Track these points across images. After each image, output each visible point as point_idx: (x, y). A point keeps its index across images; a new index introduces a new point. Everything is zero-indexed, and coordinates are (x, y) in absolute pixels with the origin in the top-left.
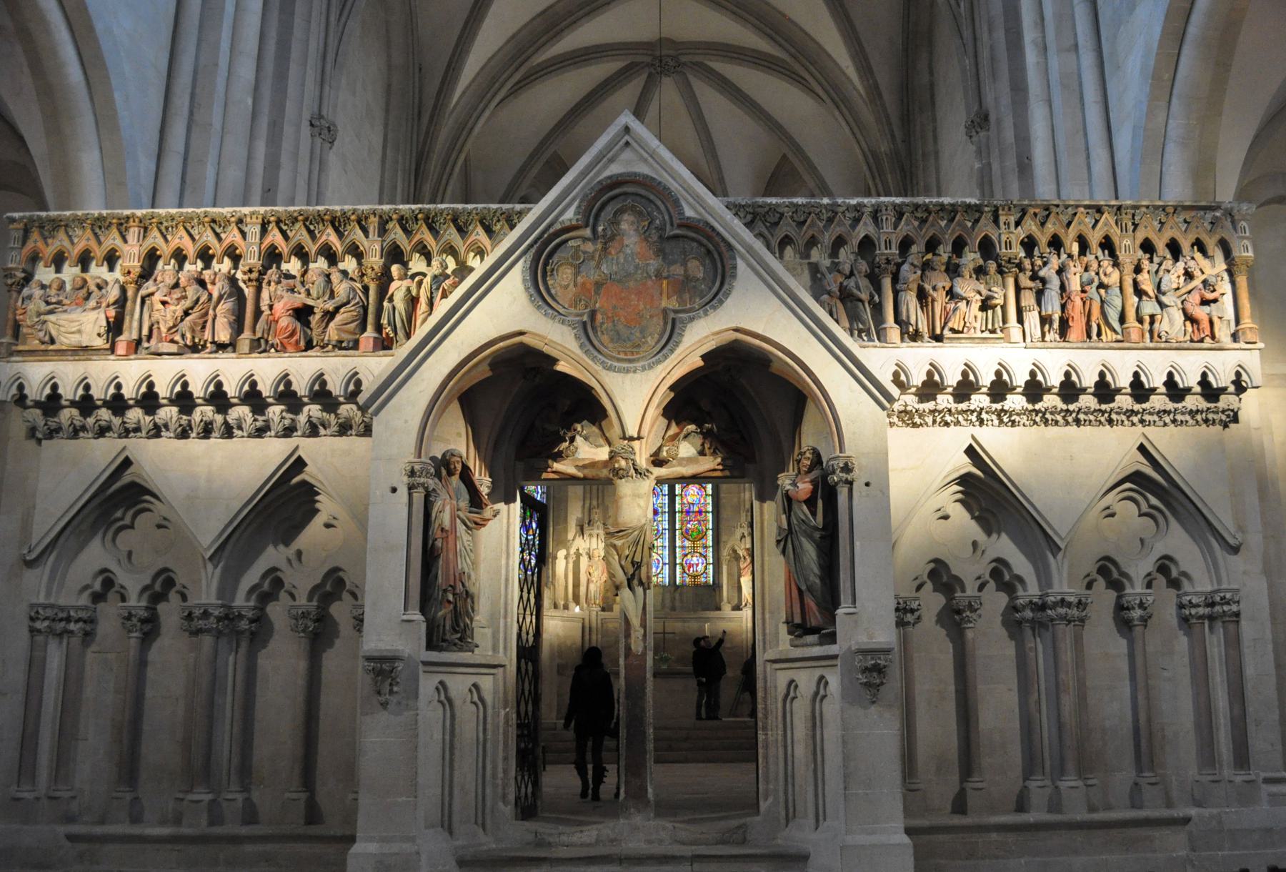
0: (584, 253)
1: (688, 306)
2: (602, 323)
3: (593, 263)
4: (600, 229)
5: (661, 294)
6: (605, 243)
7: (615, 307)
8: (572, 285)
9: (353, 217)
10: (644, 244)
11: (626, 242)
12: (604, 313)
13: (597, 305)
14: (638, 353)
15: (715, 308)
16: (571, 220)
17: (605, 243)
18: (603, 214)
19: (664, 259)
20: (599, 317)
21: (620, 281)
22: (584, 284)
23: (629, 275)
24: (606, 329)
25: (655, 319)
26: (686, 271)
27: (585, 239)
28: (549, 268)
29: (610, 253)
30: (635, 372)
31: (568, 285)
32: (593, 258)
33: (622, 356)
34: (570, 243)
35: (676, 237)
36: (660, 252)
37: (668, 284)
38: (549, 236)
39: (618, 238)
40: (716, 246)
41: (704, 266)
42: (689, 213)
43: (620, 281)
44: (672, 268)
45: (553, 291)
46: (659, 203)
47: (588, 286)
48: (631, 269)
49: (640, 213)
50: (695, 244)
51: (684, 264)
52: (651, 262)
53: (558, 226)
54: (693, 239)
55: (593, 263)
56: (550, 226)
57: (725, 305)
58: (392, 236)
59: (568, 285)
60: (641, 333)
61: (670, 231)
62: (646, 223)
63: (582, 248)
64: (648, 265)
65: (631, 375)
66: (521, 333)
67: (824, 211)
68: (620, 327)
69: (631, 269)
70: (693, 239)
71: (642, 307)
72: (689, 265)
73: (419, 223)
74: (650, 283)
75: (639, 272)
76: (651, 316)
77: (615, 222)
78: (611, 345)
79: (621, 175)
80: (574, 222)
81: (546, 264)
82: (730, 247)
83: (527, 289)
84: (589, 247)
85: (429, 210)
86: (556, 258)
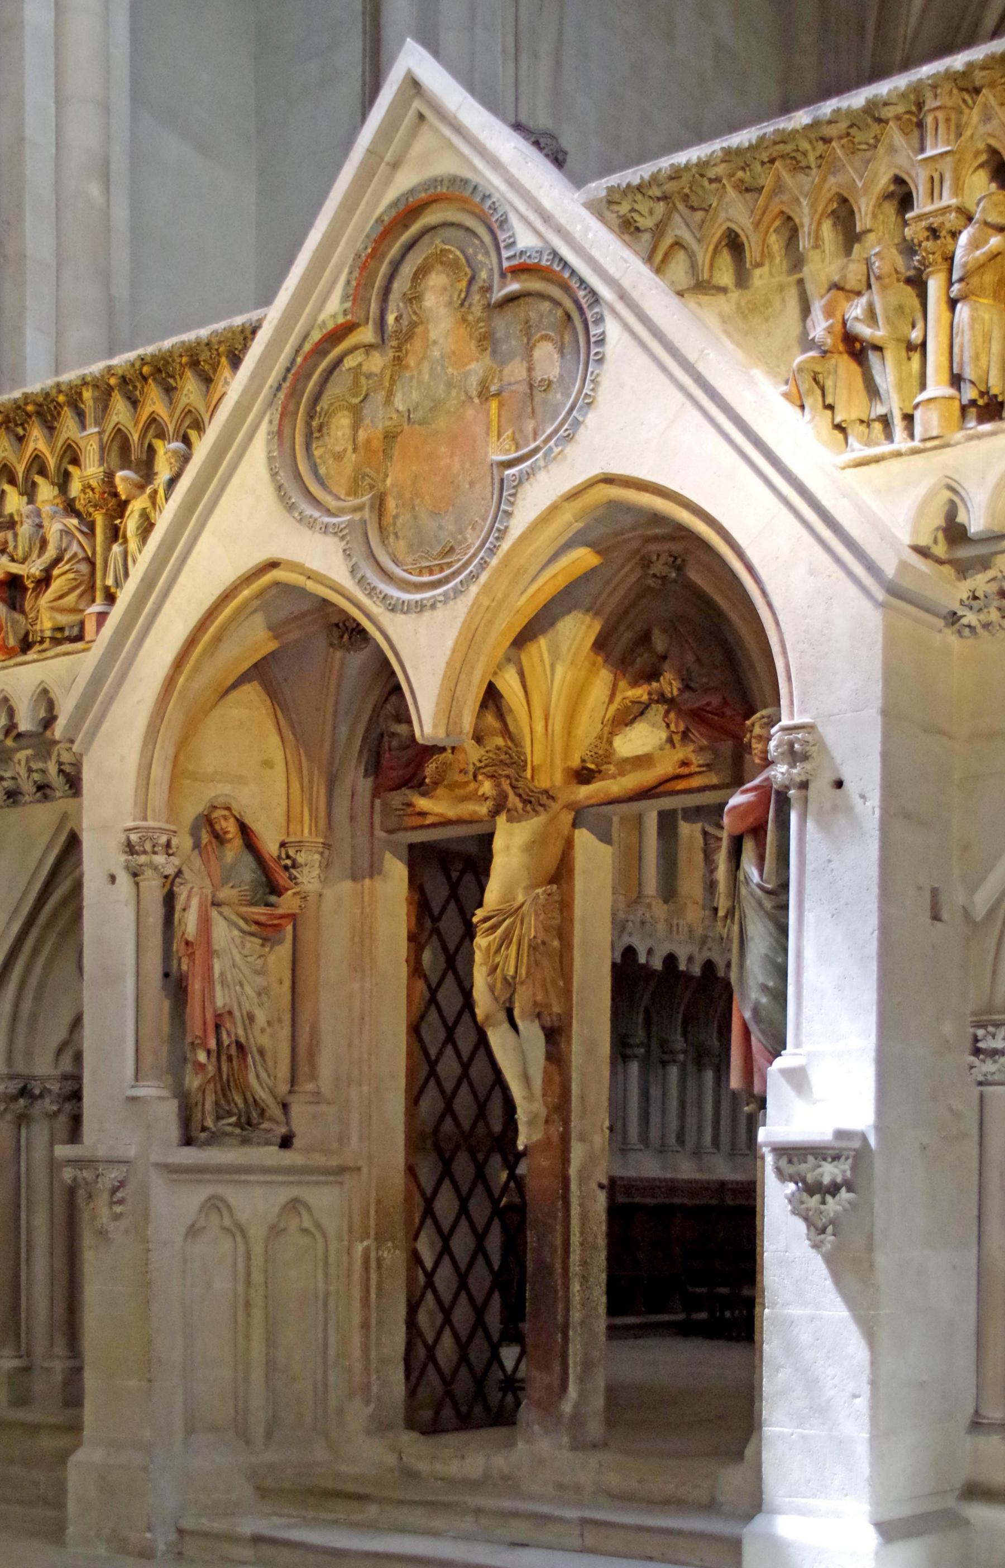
0: (368, 376)
3: (380, 397)
5: (488, 434)
6: (399, 348)
9: (61, 398)
11: (433, 336)
12: (400, 496)
14: (450, 565)
15: (569, 438)
16: (334, 316)
17: (399, 348)
19: (494, 352)
20: (391, 503)
21: (422, 422)
22: (368, 441)
23: (437, 405)
27: (369, 348)
29: (407, 367)
30: (433, 606)
31: (345, 450)
33: (426, 578)
34: (349, 362)
35: (512, 299)
36: (487, 341)
37: (501, 405)
38: (305, 359)
39: (419, 330)
42: (525, 240)
43: (422, 422)
45: (322, 470)
48: (440, 391)
50: (546, 306)
52: (473, 366)
53: (316, 336)
56: (305, 337)
59: (345, 450)
62: (464, 284)
65: (427, 615)
67: (805, 145)
69: (440, 391)
71: (456, 467)
72: (537, 354)
75: (454, 393)
76: (472, 484)
77: (414, 298)
79: (412, 191)
80: (341, 320)
82: (595, 298)
83: (274, 475)
84: (376, 363)
86: (324, 404)
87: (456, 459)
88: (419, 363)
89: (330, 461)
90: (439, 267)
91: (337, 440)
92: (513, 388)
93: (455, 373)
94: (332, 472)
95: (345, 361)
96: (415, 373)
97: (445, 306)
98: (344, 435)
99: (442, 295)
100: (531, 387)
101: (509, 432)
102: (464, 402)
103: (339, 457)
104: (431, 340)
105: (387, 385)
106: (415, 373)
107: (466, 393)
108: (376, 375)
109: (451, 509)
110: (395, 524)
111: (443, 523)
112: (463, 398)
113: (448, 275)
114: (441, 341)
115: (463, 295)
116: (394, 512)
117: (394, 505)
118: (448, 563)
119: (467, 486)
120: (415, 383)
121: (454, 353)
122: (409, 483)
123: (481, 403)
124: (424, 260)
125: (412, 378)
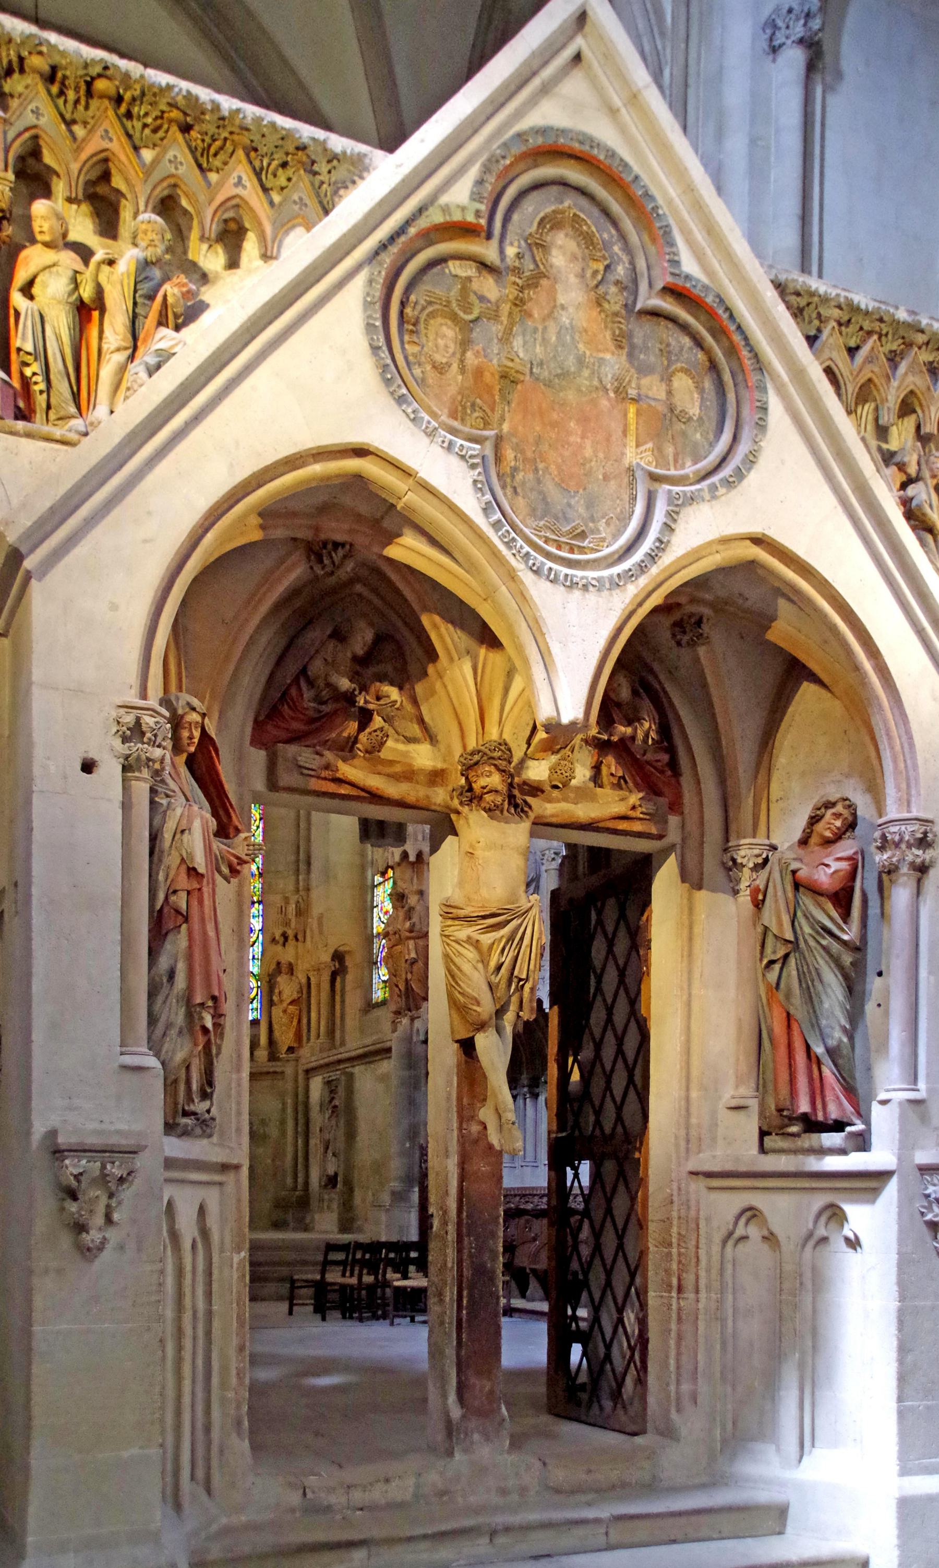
0: (482, 298)
1: (672, 472)
2: (515, 469)
3: (496, 329)
4: (511, 251)
5: (625, 433)
7: (538, 441)
8: (455, 367)
10: (595, 313)
11: (561, 299)
12: (517, 448)
13: (506, 427)
14: (582, 550)
15: (729, 484)
17: (521, 290)
18: (516, 217)
19: (631, 355)
20: (509, 454)
21: (548, 384)
22: (479, 373)
23: (564, 375)
24: (523, 483)
25: (613, 484)
26: (670, 393)
28: (408, 310)
29: (530, 315)
31: (449, 365)
32: (495, 316)
34: (454, 267)
35: (655, 314)
36: (622, 341)
37: (638, 413)
39: (544, 282)
40: (732, 352)
41: (701, 391)
43: (548, 384)
44: (645, 381)
46: (628, 225)
47: (487, 377)
49: (588, 240)
50: (687, 341)
51: (667, 379)
54: (684, 328)
55: (496, 329)
57: (745, 482)
58: (30, 119)
60: (590, 505)
61: (648, 299)
62: (601, 267)
63: (475, 285)
64: (602, 361)
66: (360, 452)
68: (550, 487)
69: (571, 363)
70: (684, 328)
71: (588, 452)
73: (94, 103)
74: (604, 403)
75: (586, 373)
76: (606, 478)
78: (530, 521)
81: (403, 304)
85: (127, 75)
87: (588, 443)
88: (544, 320)
89: (429, 367)
90: (569, 230)
91: (436, 346)
92: (653, 403)
93: (588, 353)
94: (431, 381)
95: (450, 263)
96: (540, 328)
97: (576, 276)
98: (446, 346)
99: (571, 261)
100: (672, 411)
101: (650, 445)
102: (597, 388)
103: (440, 369)
104: (558, 303)
105: (504, 319)
106: (540, 328)
107: (601, 381)
108: (489, 301)
109: (581, 491)
110: (513, 477)
111: (573, 502)
112: (596, 383)
113: (579, 245)
114: (571, 310)
115: (599, 277)
116: (513, 464)
117: (512, 456)
118: (579, 547)
119: (601, 477)
120: (539, 336)
121: (586, 331)
122: (531, 440)
123: (617, 401)
124: (554, 211)
125: (535, 330)
